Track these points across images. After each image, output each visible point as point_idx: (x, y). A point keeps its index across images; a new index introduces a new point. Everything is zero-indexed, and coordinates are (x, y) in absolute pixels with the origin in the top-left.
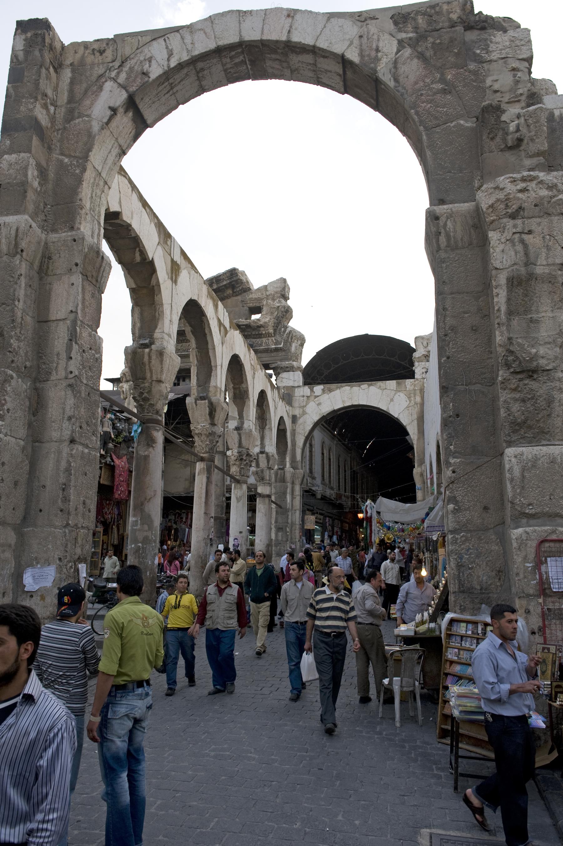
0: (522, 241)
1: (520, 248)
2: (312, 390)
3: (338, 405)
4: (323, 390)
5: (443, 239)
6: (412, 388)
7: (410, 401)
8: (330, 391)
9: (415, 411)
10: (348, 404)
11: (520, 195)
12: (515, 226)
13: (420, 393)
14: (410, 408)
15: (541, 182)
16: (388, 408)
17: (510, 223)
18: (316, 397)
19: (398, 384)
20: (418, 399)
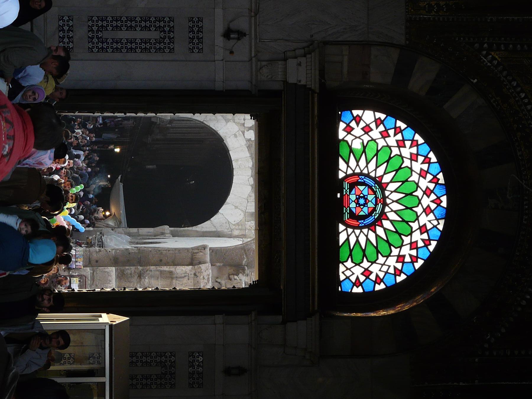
0: (185, 276)
1: (183, 275)
2: (250, 128)
3: (233, 155)
4: (250, 140)
5: (196, 251)
6: (248, 227)
7: (234, 225)
8: (249, 147)
9: (225, 229)
10: (234, 164)
11: (202, 277)
12: (191, 274)
13: (242, 235)
14: (228, 225)
15: (207, 284)
16: (228, 204)
17: (193, 273)
18: (243, 133)
19: (251, 214)
20: (236, 233)
